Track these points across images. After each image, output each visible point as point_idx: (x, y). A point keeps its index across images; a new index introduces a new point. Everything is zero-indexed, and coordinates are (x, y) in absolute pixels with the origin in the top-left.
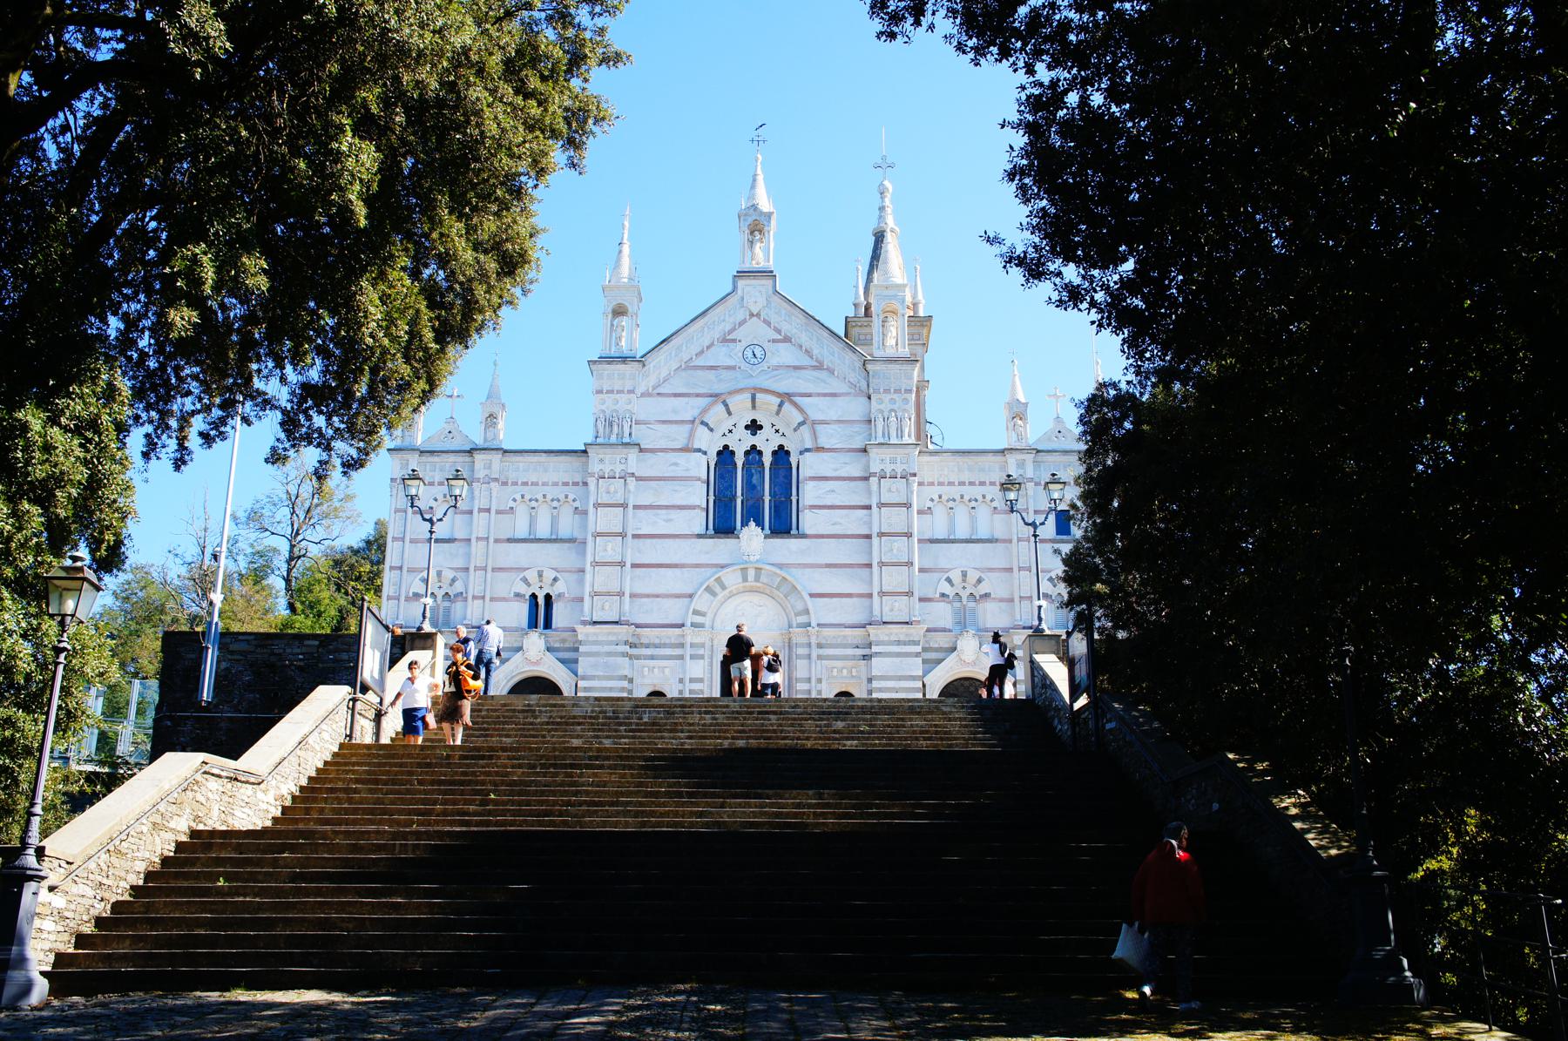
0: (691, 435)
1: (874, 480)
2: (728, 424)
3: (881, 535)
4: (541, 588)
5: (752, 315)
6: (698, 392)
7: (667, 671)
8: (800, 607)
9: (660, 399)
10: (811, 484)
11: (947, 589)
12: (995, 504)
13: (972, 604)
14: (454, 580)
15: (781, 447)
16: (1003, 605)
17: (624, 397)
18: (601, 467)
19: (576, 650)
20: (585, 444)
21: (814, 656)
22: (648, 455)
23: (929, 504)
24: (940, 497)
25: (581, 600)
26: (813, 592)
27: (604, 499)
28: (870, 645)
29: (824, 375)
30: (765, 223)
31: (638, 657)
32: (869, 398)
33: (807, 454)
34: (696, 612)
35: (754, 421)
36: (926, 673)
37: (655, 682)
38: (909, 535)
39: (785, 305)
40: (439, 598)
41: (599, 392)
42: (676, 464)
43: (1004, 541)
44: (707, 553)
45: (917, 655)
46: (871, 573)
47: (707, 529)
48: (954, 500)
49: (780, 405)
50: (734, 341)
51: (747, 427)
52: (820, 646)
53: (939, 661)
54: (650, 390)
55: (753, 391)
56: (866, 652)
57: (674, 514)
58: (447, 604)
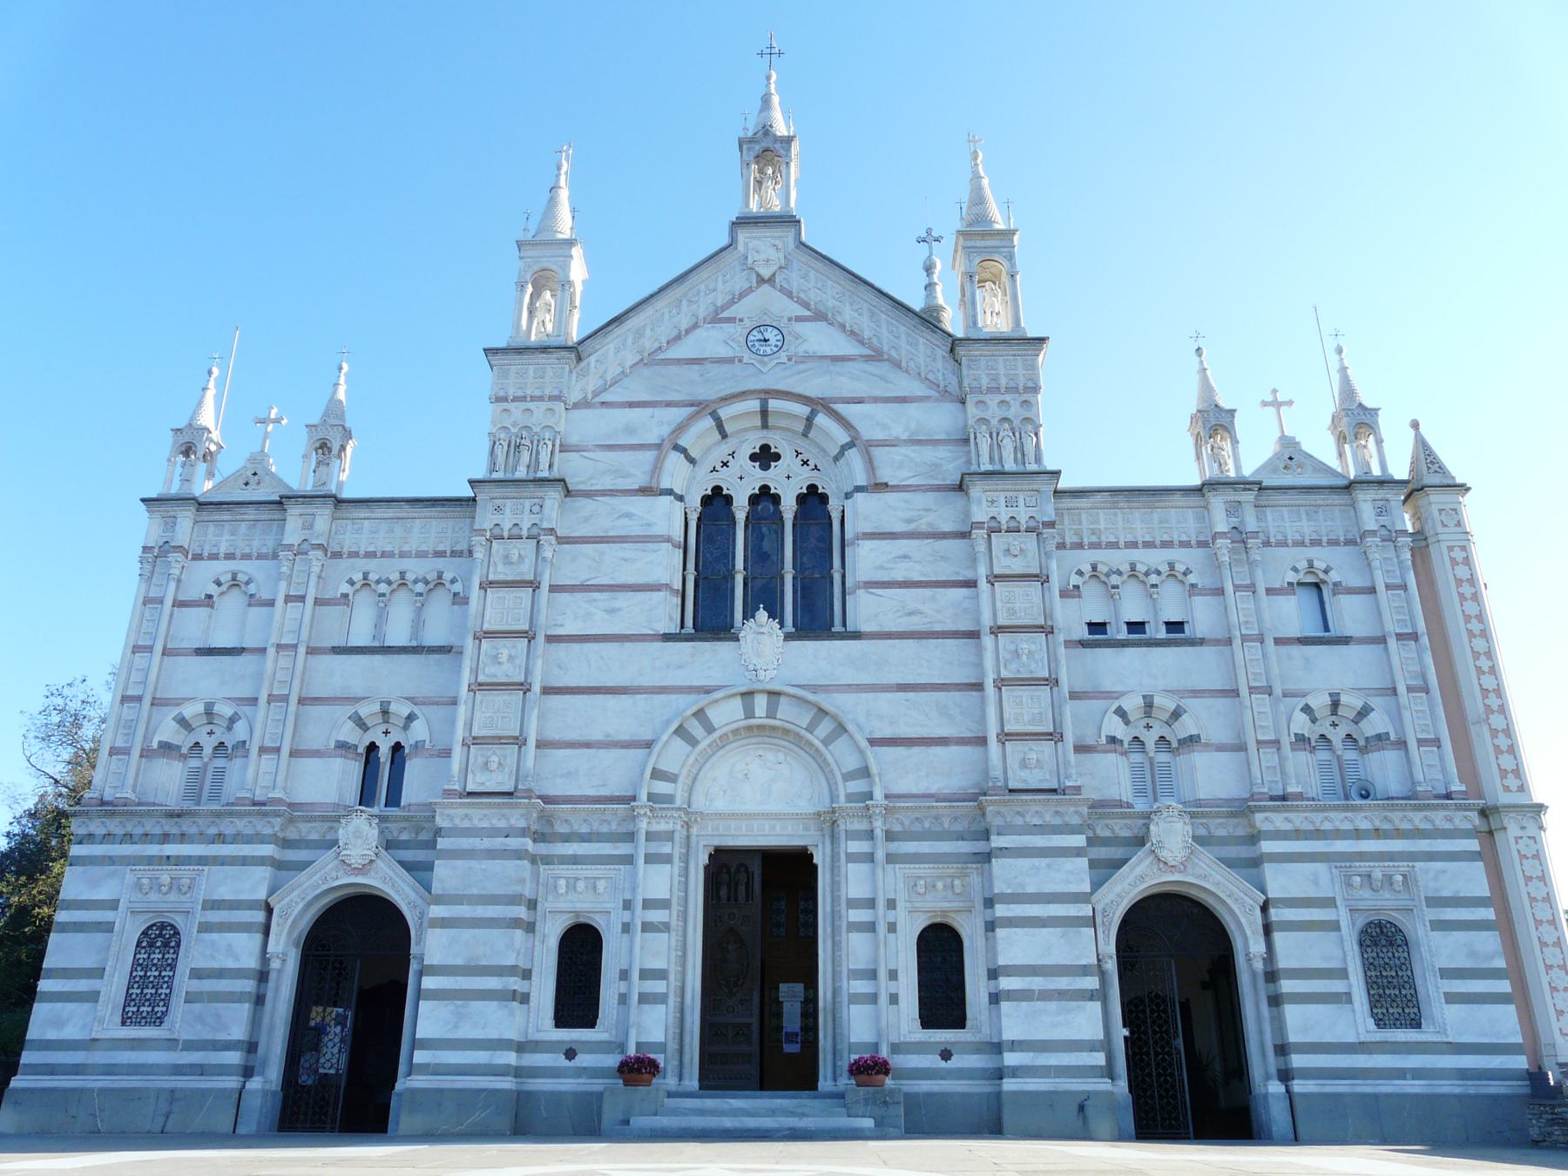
0: (657, 467)
1: (979, 534)
2: (723, 450)
3: (997, 630)
4: (386, 733)
5: (761, 281)
6: (669, 398)
7: (601, 885)
8: (852, 763)
9: (605, 410)
10: (866, 546)
11: (1114, 726)
12: (1192, 579)
13: (1163, 757)
14: (232, 720)
15: (812, 488)
16: (1224, 757)
17: (539, 408)
18: (497, 518)
19: (432, 844)
20: (473, 483)
21: (880, 855)
22: (582, 502)
23: (1075, 580)
24: (1094, 568)
25: (446, 753)
26: (878, 735)
27: (500, 572)
28: (986, 835)
29: (884, 368)
30: (782, 152)
31: (548, 860)
32: (963, 402)
33: (859, 496)
34: (657, 774)
35: (765, 448)
36: (1097, 885)
37: (579, 906)
38: (1048, 631)
39: (819, 265)
40: (208, 751)
41: (505, 399)
43: (1216, 642)
44: (680, 667)
45: (1078, 852)
46: (983, 701)
47: (682, 627)
48: (1120, 573)
49: (809, 421)
51: (753, 457)
52: (890, 836)
53: (1118, 864)
54: (590, 396)
55: (763, 396)
56: (980, 846)
57: (622, 600)
58: (220, 763)
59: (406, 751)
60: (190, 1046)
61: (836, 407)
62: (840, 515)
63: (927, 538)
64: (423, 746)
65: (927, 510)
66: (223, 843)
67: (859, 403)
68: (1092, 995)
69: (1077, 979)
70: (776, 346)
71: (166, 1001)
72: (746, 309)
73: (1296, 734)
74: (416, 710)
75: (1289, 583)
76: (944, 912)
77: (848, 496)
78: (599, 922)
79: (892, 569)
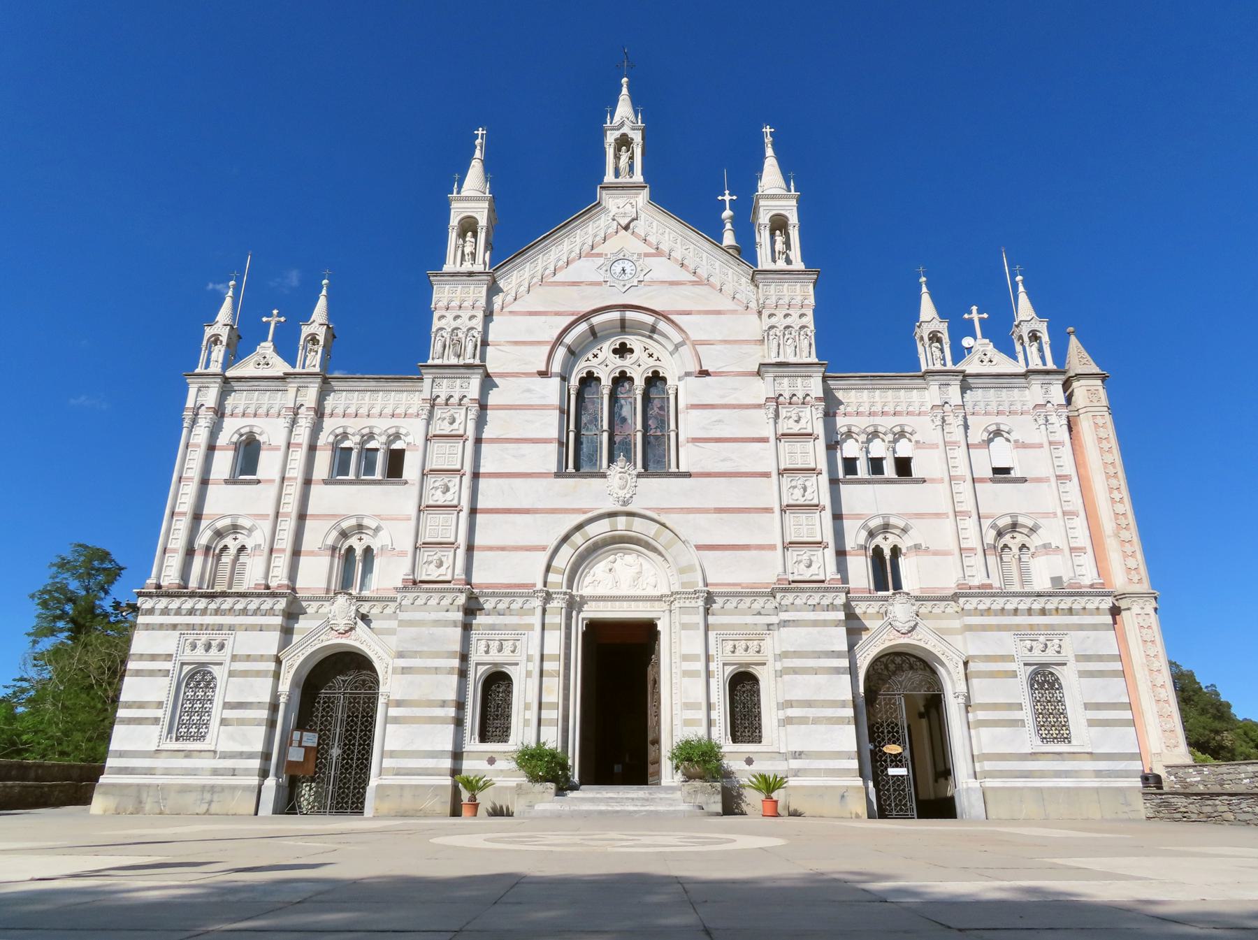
4: (360, 539)
15: (656, 373)
33: (688, 378)
35: (623, 345)
42: (529, 390)
50: (599, 255)
51: (615, 351)
56: (774, 620)
59: (375, 552)
60: (225, 756)
61: (672, 317)
62: (674, 392)
63: (735, 408)
64: (387, 548)
65: (735, 389)
66: (247, 615)
67: (688, 314)
68: (849, 721)
69: (839, 710)
70: (631, 274)
71: (207, 725)
72: (610, 247)
73: (987, 544)
74: (383, 523)
75: (983, 441)
76: (749, 665)
77: (680, 379)
78: (509, 670)
79: (711, 429)
